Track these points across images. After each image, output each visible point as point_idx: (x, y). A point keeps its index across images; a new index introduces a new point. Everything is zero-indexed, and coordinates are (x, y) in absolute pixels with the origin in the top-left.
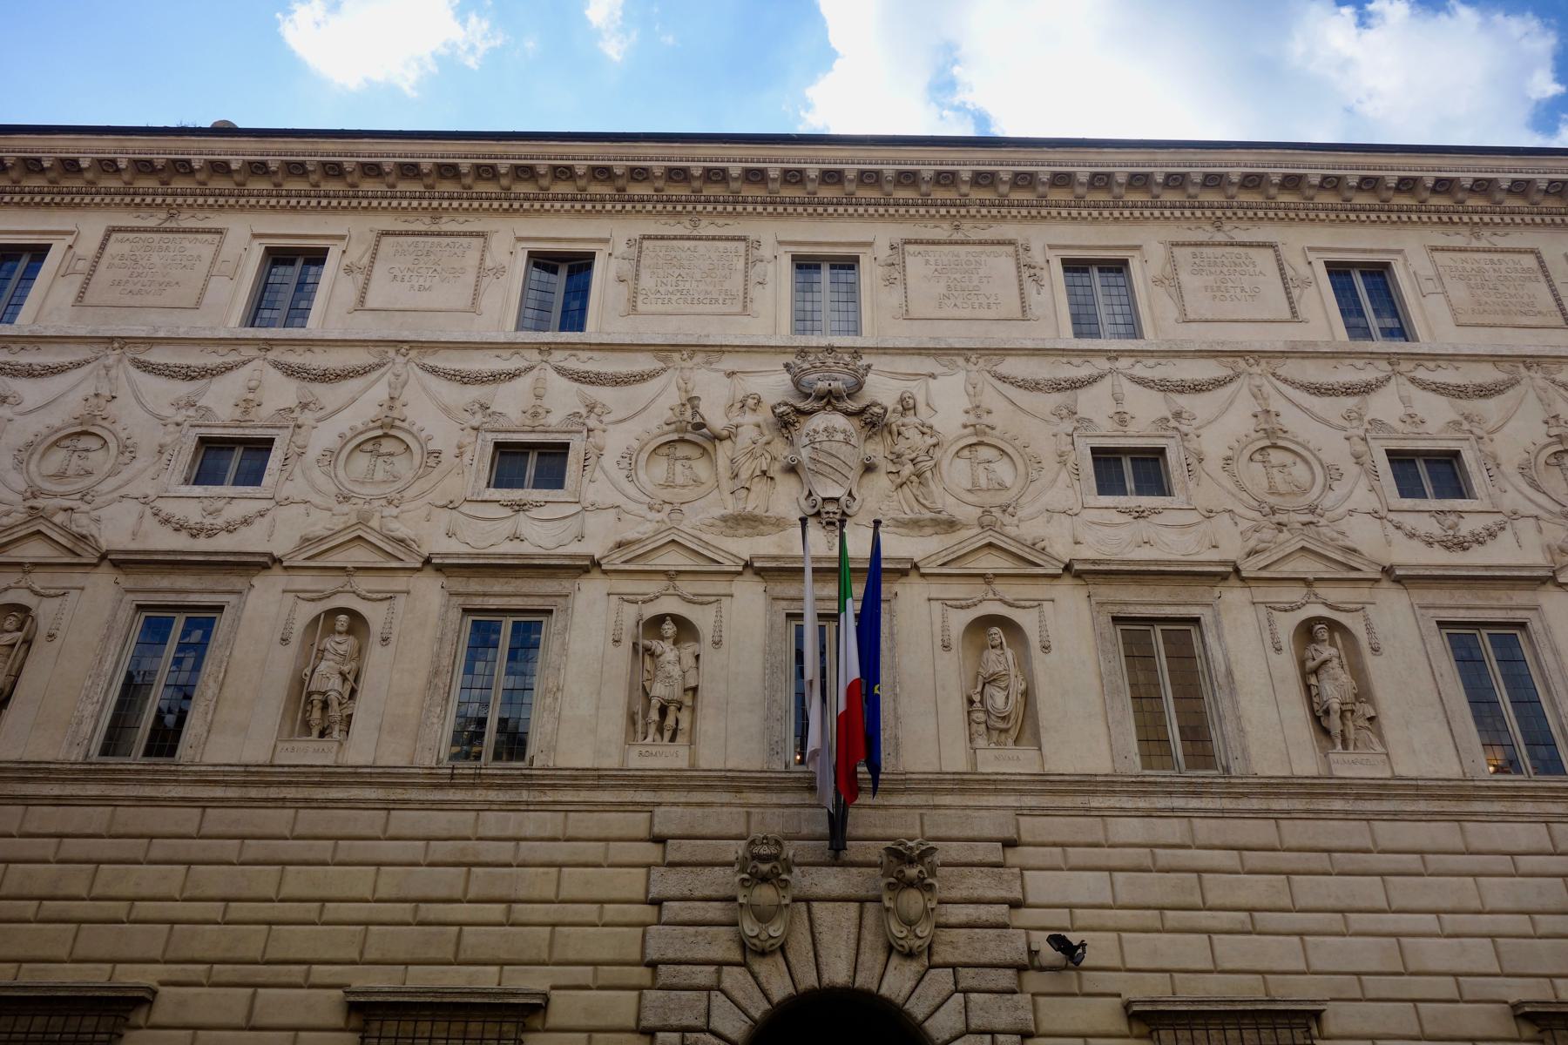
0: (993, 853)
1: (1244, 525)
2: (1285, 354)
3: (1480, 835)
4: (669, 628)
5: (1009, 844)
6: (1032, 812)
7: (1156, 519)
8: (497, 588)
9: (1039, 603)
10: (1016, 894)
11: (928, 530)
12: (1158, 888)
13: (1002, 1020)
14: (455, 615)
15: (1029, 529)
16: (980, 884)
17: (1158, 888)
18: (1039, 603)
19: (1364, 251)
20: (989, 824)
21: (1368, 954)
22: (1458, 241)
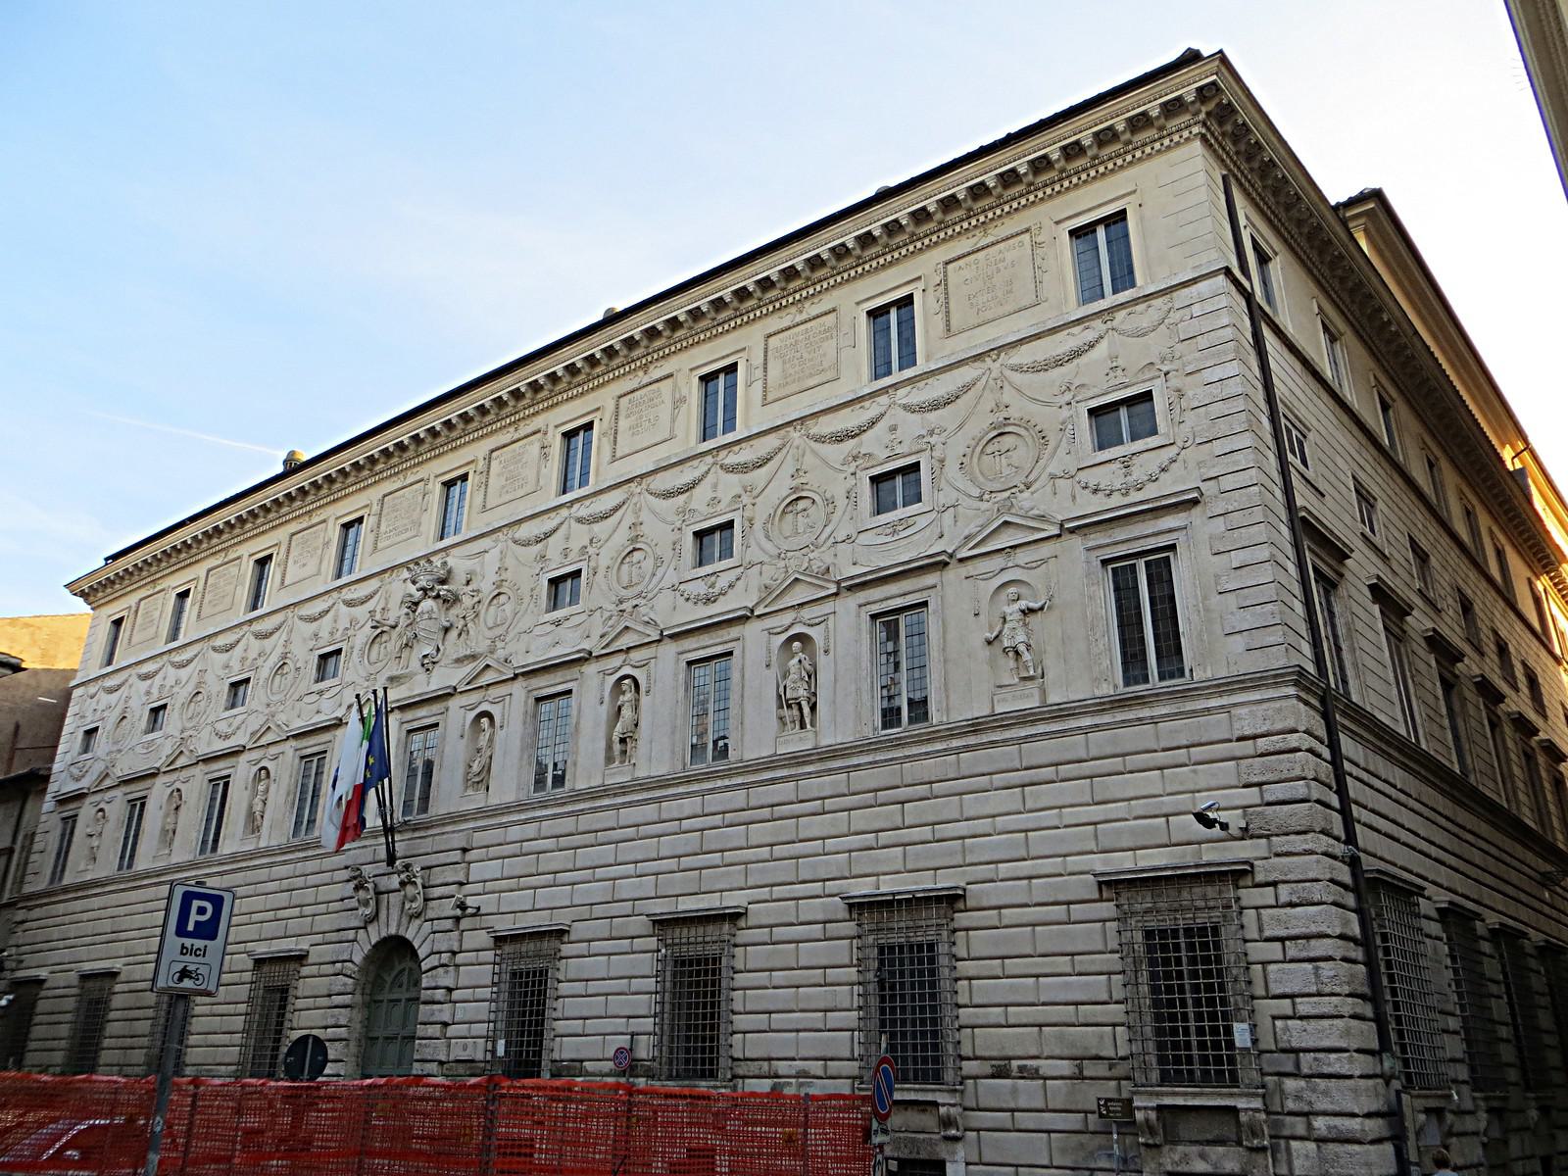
0: (456, 856)
1: (606, 614)
3: (671, 808)
5: (465, 850)
6: (475, 830)
7: (567, 624)
10: (461, 878)
12: (517, 865)
14: (297, 760)
16: (450, 875)
17: (517, 865)
19: (723, 357)
20: (458, 841)
21: (597, 891)
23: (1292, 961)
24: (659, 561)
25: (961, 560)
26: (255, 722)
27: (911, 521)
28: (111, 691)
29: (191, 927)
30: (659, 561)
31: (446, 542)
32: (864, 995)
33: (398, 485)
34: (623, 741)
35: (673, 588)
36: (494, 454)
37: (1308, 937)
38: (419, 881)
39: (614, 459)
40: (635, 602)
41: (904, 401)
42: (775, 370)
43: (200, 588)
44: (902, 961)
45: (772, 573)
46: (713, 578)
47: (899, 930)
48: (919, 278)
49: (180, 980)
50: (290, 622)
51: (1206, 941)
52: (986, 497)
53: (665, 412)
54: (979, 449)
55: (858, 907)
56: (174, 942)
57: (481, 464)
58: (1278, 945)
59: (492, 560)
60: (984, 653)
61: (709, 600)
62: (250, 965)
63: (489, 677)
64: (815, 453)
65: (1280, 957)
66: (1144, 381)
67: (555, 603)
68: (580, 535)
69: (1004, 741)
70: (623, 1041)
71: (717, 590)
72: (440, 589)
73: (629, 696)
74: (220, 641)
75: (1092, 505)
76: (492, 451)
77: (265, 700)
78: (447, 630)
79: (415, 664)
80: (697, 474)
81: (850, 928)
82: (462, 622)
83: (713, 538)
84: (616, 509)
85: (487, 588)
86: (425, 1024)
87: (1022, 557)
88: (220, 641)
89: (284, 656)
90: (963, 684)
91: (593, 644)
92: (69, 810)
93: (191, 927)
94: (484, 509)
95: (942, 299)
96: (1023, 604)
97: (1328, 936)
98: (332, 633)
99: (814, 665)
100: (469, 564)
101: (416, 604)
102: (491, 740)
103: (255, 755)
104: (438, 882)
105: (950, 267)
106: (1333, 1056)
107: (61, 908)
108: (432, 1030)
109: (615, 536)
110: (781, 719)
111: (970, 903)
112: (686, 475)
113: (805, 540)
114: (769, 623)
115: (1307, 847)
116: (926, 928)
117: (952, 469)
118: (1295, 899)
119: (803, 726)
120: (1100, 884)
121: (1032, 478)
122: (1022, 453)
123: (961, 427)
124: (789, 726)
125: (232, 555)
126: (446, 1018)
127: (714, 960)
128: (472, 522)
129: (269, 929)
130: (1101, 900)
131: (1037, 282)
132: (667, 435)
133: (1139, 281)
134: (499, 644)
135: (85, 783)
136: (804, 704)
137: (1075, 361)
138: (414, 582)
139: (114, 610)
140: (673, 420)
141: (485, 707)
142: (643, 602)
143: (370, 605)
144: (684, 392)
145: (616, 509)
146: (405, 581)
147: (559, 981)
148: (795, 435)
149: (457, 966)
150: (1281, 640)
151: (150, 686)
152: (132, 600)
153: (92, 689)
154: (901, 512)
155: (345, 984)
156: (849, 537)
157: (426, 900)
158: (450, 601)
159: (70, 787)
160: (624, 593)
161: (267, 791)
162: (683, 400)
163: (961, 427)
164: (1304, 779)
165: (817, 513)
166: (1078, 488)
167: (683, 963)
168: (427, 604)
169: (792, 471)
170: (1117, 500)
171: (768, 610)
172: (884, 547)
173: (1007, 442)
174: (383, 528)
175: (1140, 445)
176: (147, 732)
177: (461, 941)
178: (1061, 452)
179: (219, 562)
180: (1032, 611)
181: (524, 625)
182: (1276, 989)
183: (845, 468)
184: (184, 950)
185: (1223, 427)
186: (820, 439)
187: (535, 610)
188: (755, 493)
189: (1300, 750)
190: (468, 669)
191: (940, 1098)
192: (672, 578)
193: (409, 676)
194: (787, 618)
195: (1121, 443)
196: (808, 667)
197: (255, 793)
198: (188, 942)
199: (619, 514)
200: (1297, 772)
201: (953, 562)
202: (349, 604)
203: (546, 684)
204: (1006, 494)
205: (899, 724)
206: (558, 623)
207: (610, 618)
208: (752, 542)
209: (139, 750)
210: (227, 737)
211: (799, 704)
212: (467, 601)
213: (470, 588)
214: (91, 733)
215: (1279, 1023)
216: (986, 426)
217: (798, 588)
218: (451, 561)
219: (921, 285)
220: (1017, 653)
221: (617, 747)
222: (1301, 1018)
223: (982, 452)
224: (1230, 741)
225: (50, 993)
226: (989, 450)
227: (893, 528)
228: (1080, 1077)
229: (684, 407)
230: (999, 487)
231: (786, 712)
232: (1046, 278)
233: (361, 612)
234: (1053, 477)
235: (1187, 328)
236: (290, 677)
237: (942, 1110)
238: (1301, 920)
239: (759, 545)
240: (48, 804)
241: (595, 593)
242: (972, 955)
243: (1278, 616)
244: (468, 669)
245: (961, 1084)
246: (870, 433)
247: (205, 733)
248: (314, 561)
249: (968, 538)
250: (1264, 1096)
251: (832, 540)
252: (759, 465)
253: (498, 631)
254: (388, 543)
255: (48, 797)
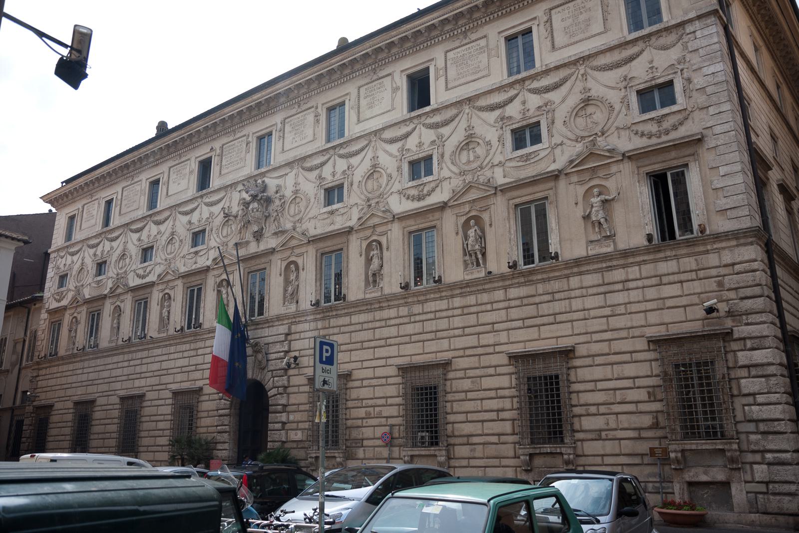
0: (282, 338)
1: (360, 207)
2: (383, 129)
4: (224, 283)
7: (337, 213)
8: (193, 280)
9: (303, 254)
10: (286, 348)
11: (279, 235)
13: (280, 383)
15: (304, 227)
16: (278, 347)
18: (303, 254)
22: (457, 43)
23: (754, 377)
24: (390, 176)
25: (566, 174)
26: (159, 270)
27: (536, 154)
28: (73, 254)
29: (324, 359)
30: (390, 176)
31: (263, 170)
32: (520, 402)
33: (231, 138)
34: (374, 275)
35: (400, 192)
36: (287, 121)
37: (762, 365)
38: (263, 351)
39: (359, 121)
40: (376, 200)
41: (529, 87)
42: (452, 73)
43: (119, 197)
44: (540, 384)
45: (457, 182)
46: (422, 187)
47: (539, 369)
48: (535, 18)
49: (323, 385)
50: (173, 215)
51: (705, 367)
52: (579, 140)
53: (387, 94)
54: (574, 113)
55: (514, 358)
56: (319, 366)
57: (279, 125)
58: (746, 370)
59: (290, 181)
60: (582, 222)
61: (420, 198)
62: (170, 395)
63: (294, 243)
64: (479, 117)
65: (747, 375)
66: (669, 75)
67: (329, 202)
68: (342, 165)
69: (594, 270)
70: (387, 429)
71: (425, 192)
72: (261, 197)
73: (375, 252)
74: (134, 227)
75: (639, 143)
76: (286, 119)
77: (164, 258)
78: (267, 217)
79: (249, 236)
80: (409, 129)
81: (511, 369)
82: (276, 214)
83: (420, 167)
84: (362, 150)
85: (288, 193)
86: (273, 423)
87: (601, 173)
88: (134, 227)
89: (173, 234)
90: (568, 237)
91: (353, 222)
92: (56, 318)
93: (324, 359)
94: (283, 151)
95: (549, 29)
96: (603, 197)
97: (773, 364)
98: (200, 221)
99: (483, 231)
100: (277, 182)
101: (249, 204)
102: (297, 277)
103: (161, 287)
104: (274, 351)
105: (553, 12)
106: (776, 423)
107: (55, 369)
108: (279, 426)
109: (361, 165)
110: (465, 261)
111: (577, 354)
112: (404, 130)
113: (474, 165)
114: (456, 210)
115: (761, 320)
116: (555, 367)
117: (559, 123)
118: (755, 346)
119: (478, 265)
120: (649, 342)
121: (605, 129)
122: (599, 116)
123: (563, 101)
124: (470, 265)
125: (136, 180)
126: (284, 419)
127: (435, 388)
128: (277, 157)
129: (179, 377)
130: (649, 350)
131: (605, 20)
132: (389, 108)
133: (665, 19)
134: (298, 225)
135: (64, 303)
136: (478, 253)
137: (628, 65)
138: (247, 192)
139: (70, 210)
140: (393, 100)
141: (293, 259)
142: (382, 200)
143: (221, 205)
144: (399, 84)
145: (362, 150)
146: (240, 192)
147: (347, 400)
148: (467, 109)
149: (288, 394)
150: (748, 213)
151: (96, 251)
152: (79, 205)
153: (62, 254)
154: (530, 149)
155: (225, 404)
156: (500, 162)
157: (267, 361)
158: (269, 201)
159: (54, 305)
160: (370, 196)
161: (169, 306)
162: (398, 88)
163: (563, 101)
164: (760, 285)
165: (480, 151)
166: (632, 135)
167: (418, 389)
168: (255, 205)
169: (465, 126)
170: (654, 140)
171: (455, 203)
172: (522, 168)
173: (590, 109)
174: (224, 163)
175: (666, 110)
176: (96, 276)
177: (289, 381)
178: (621, 116)
179: (129, 183)
180: (607, 201)
181: (310, 215)
182: (745, 391)
183: (497, 125)
184: (324, 371)
185: (714, 99)
186: (481, 109)
187: (318, 209)
188: (443, 140)
189: (758, 270)
190: (281, 239)
191: (564, 450)
192: (397, 187)
193: (248, 243)
194: (467, 208)
195: (655, 109)
196: (480, 234)
197: (162, 307)
198: (325, 366)
199: (363, 153)
200: (757, 282)
201: (562, 177)
202: (207, 205)
203: (329, 245)
204: (591, 138)
205: (533, 262)
206: (332, 213)
207: (362, 209)
208: (444, 165)
209: (94, 285)
210: (143, 277)
211: (476, 253)
212: (277, 202)
213: (278, 195)
214: (63, 278)
215: (746, 408)
216: (578, 101)
217: (473, 191)
218: (267, 180)
219: (536, 22)
220: (600, 223)
221: (371, 279)
222: (759, 405)
223: (576, 114)
224: (720, 267)
225: (148, 403)
226: (581, 113)
227: (527, 157)
228: (640, 438)
229: (399, 93)
230: (587, 134)
231: (467, 258)
232: (609, 17)
233: (216, 209)
234: (618, 128)
235: (692, 46)
236: (177, 245)
237: (566, 457)
238: (759, 356)
239: (448, 167)
240: (44, 315)
241: (354, 198)
242: (579, 380)
243: (746, 201)
244: (281, 239)
245: (575, 443)
246: (510, 105)
247: (131, 276)
248: (186, 181)
249: (571, 162)
250: (738, 443)
251: (490, 165)
252: (446, 123)
253: (297, 218)
254: (226, 171)
255: (43, 311)
